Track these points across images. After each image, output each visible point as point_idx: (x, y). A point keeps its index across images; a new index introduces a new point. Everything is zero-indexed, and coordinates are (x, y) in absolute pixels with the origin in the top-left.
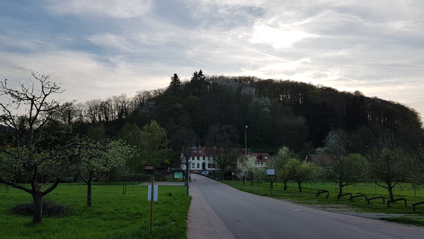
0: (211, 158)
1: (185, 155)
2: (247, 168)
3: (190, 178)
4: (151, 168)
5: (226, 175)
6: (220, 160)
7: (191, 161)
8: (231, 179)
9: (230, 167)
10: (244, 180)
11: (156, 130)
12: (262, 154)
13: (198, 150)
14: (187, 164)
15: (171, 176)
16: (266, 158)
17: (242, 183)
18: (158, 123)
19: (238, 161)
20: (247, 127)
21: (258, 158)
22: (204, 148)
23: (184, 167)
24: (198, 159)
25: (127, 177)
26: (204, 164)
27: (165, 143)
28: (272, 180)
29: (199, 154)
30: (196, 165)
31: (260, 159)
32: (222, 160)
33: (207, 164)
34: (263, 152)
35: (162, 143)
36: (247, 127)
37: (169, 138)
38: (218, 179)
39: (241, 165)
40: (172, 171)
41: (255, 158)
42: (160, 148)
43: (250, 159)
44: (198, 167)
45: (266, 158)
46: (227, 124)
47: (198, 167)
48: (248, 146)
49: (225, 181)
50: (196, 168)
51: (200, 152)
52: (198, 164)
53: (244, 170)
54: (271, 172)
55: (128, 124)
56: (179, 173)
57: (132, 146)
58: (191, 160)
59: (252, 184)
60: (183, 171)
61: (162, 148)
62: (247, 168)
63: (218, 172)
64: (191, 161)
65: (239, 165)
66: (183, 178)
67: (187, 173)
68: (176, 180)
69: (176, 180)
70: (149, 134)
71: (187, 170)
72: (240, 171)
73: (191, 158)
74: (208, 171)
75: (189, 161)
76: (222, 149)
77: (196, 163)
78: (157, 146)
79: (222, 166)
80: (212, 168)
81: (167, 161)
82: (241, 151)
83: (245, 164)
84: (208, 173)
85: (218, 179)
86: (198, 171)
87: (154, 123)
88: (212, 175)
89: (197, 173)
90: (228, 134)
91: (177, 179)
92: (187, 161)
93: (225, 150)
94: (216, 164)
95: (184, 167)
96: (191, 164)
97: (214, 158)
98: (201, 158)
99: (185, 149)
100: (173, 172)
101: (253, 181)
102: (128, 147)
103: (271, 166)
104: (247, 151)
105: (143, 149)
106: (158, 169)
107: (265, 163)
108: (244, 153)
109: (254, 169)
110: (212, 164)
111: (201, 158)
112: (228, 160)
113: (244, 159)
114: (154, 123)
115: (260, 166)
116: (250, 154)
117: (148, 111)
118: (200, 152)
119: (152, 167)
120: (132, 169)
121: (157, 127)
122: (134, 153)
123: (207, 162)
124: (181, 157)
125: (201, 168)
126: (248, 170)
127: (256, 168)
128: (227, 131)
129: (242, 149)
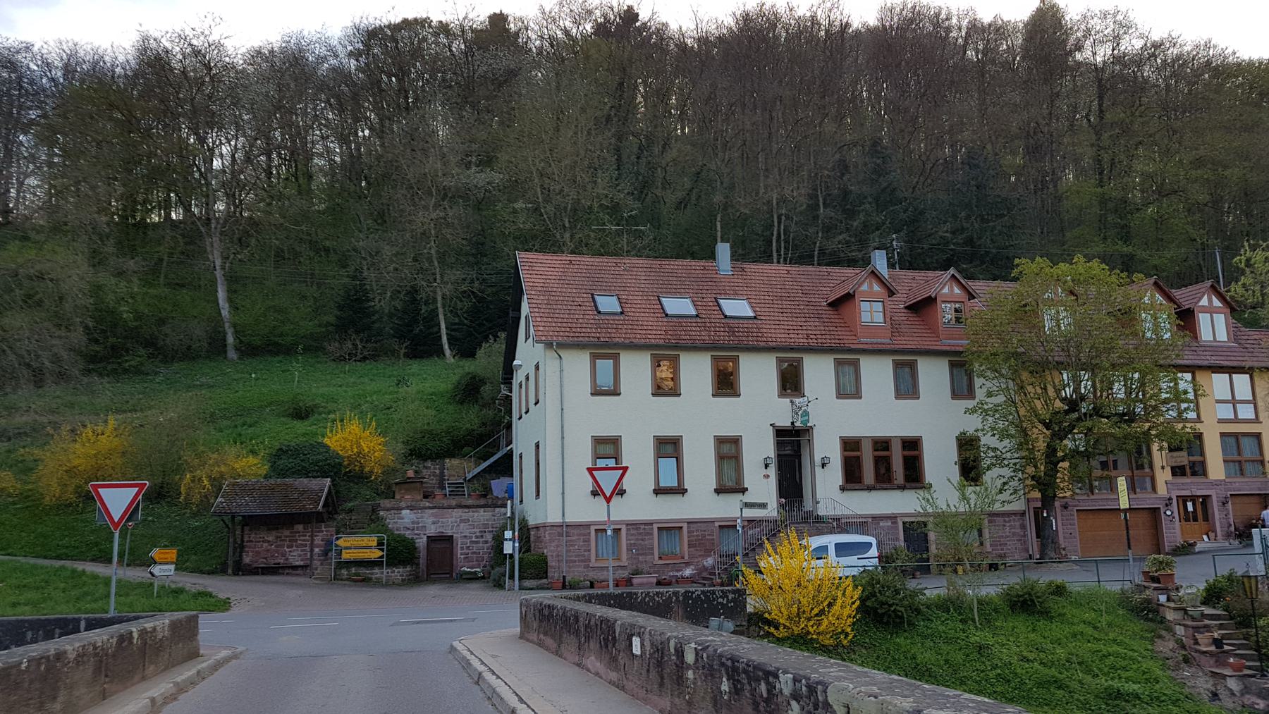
24: (726, 383)
30: (700, 467)
33: (825, 447)
44: (730, 485)
47: (730, 485)
51: (737, 307)
52: (729, 451)
98: (759, 373)
111: (759, 373)
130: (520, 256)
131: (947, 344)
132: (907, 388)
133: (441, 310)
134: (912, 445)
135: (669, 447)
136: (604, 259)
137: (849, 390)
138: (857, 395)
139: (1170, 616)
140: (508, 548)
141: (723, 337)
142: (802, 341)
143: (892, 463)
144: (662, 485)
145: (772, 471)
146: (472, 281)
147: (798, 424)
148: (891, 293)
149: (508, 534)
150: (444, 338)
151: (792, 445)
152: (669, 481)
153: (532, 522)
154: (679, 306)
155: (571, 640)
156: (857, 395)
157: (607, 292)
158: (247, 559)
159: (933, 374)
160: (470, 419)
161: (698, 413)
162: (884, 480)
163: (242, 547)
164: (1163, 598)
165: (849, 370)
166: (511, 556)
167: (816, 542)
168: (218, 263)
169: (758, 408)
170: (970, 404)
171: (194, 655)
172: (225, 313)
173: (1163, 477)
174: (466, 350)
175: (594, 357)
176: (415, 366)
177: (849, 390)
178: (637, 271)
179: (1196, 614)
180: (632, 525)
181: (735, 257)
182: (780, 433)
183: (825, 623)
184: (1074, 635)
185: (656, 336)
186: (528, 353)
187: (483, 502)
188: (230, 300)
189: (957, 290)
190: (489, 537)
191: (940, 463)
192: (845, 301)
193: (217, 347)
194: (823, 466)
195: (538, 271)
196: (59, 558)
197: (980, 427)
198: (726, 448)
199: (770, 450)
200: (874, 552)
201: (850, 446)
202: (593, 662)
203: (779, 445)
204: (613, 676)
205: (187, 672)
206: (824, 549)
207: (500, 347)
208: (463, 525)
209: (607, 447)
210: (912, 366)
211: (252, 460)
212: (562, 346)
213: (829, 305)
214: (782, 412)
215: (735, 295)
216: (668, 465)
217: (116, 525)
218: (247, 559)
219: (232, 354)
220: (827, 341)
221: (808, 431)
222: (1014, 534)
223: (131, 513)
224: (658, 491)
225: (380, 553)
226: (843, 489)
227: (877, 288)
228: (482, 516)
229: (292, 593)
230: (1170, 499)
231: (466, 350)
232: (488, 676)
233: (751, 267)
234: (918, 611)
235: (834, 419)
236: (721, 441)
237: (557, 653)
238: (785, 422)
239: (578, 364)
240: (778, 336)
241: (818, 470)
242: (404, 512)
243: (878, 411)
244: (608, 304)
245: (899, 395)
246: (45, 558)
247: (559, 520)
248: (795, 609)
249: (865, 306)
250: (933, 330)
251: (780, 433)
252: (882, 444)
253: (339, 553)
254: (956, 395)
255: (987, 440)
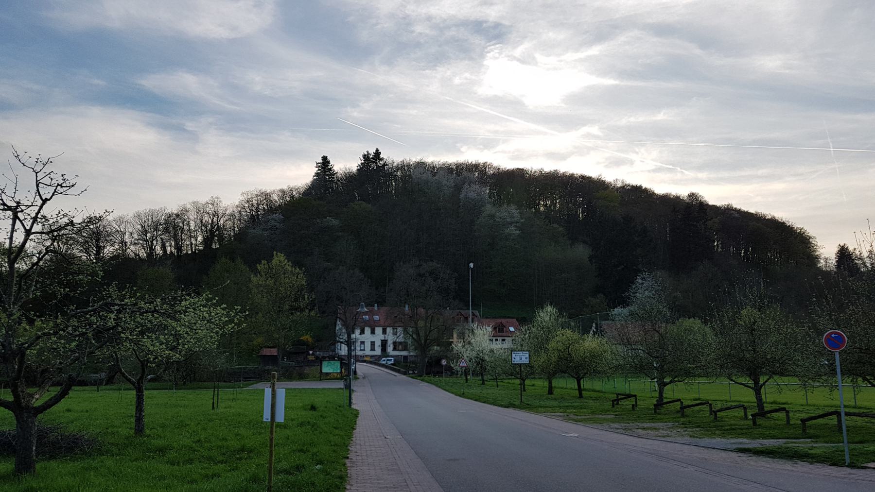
0: (400, 330)
1: (345, 324)
2: (472, 350)
3: (355, 373)
4: (274, 352)
5: (430, 364)
6: (418, 335)
7: (358, 336)
8: (439, 373)
9: (438, 348)
10: (466, 373)
11: (284, 274)
12: (504, 321)
13: (371, 313)
14: (350, 343)
15: (314, 370)
16: (512, 329)
17: (462, 380)
18: (288, 257)
19: (455, 336)
20: (472, 265)
21: (495, 328)
22: (384, 309)
23: (343, 350)
24: (373, 332)
25: (221, 371)
26: (384, 344)
27: (304, 298)
28: (524, 375)
29: (375, 321)
30: (368, 346)
31: (500, 331)
32: (422, 334)
34: (505, 317)
35: (296, 300)
36: (472, 265)
37: (311, 289)
38: (414, 373)
39: (460, 345)
40: (317, 358)
41: (490, 329)
42: (294, 309)
43: (479, 332)
44: (373, 349)
45: (512, 329)
46: (432, 261)
47: (373, 349)
48: (475, 306)
49: (427, 378)
50: (368, 352)
51: (377, 318)
52: (373, 344)
53: (467, 353)
54: (521, 358)
55: (223, 260)
56: (332, 362)
57: (230, 307)
58: (356, 334)
59: (483, 384)
60: (341, 359)
61: (296, 309)
62: (472, 350)
63: (413, 359)
64: (358, 336)
65: (457, 345)
66: (341, 372)
67: (349, 361)
68: (327, 377)
69: (327, 377)
70: (270, 282)
71: (349, 355)
72: (458, 357)
73: (358, 332)
74: (392, 356)
75: (353, 336)
76: (421, 310)
77: (368, 340)
78: (287, 307)
79: (422, 346)
80: (402, 350)
81: (307, 338)
82: (461, 315)
83: (469, 343)
84: (392, 362)
85: (414, 373)
86: (372, 356)
87: (279, 258)
88: (402, 366)
89: (371, 362)
90: (434, 281)
91: (327, 374)
92: (349, 336)
93: (427, 313)
94: (409, 342)
95: (343, 350)
96: (358, 344)
97: (405, 331)
98: (379, 330)
99: (345, 312)
100: (320, 361)
101: (485, 378)
102: (223, 309)
103: (522, 345)
104: (473, 314)
105: (257, 313)
106: (289, 355)
107: (510, 339)
108: (466, 318)
109: (487, 351)
110: (400, 343)
111: (379, 330)
112: (434, 334)
113: (467, 331)
114: (279, 258)
115: (500, 346)
116: (479, 322)
117: (266, 234)
118: (377, 318)
119: (276, 350)
120: (232, 354)
121: (287, 267)
122: (236, 321)
123: (391, 338)
124: (337, 328)
125: (378, 351)
126: (474, 354)
127: (492, 351)
128: (431, 273)
129: (463, 312)
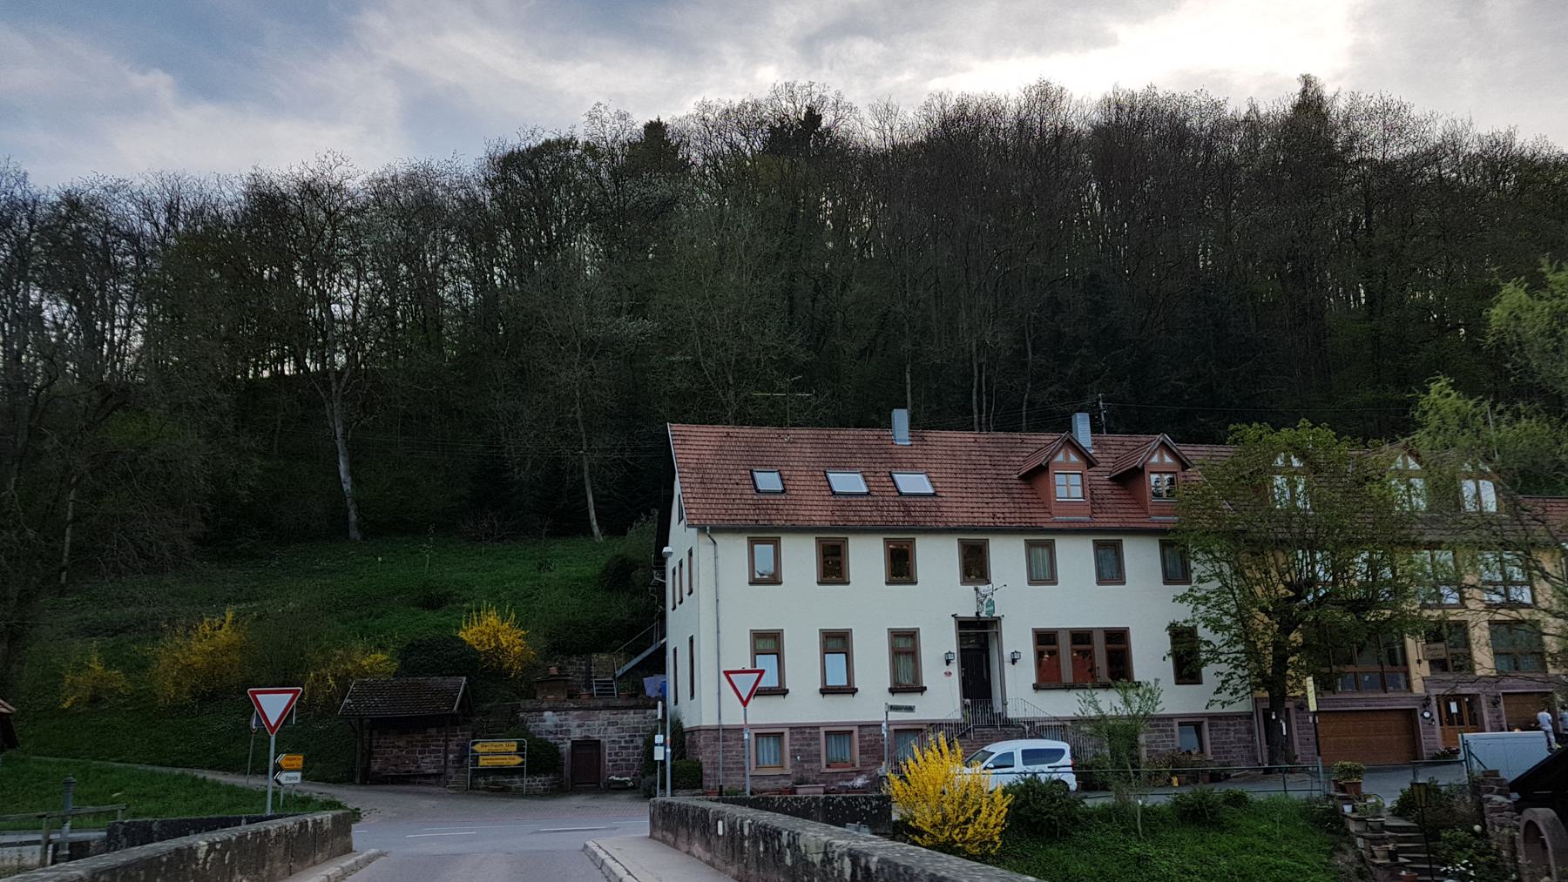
24: (901, 568)
26: (977, 638)
30: (872, 664)
33: (1016, 640)
44: (907, 683)
47: (907, 683)
51: (913, 483)
52: (905, 645)
98: (937, 558)
111: (937, 558)
125: (942, 697)
130: (672, 428)
131: (1157, 520)
132: (1110, 571)
133: (587, 481)
134: (1118, 639)
135: (837, 641)
136: (765, 430)
137: (1043, 574)
138: (1052, 580)
139: (1353, 827)
140: (659, 754)
141: (898, 516)
142: (987, 520)
143: (1094, 657)
144: (829, 683)
145: (955, 668)
146: (622, 450)
147: (983, 615)
148: (1090, 463)
149: (659, 739)
150: (592, 513)
151: (977, 638)
152: (837, 678)
153: (686, 725)
154: (848, 482)
155: (683, 831)
156: (1052, 580)
157: (768, 467)
158: (375, 767)
159: (1141, 557)
160: (621, 608)
161: (868, 601)
162: (1085, 679)
163: (370, 753)
164: (1348, 809)
165: (1042, 553)
166: (663, 763)
167: (998, 748)
168: (339, 431)
169: (938, 596)
170: (1182, 589)
171: (348, 850)
172: (347, 487)
173: (1420, 671)
174: (615, 526)
175: (752, 542)
176: (558, 547)
177: (1043, 574)
178: (801, 442)
179: (1376, 826)
180: (796, 729)
181: (914, 424)
182: (963, 624)
183: (970, 832)
184: (1245, 848)
185: (820, 517)
186: (681, 539)
187: (633, 702)
188: (351, 472)
189: (1168, 459)
190: (639, 741)
191: (1150, 658)
192: (1036, 476)
193: (337, 529)
194: (1014, 661)
195: (693, 445)
196: (175, 765)
197: (1190, 617)
198: (902, 643)
199: (952, 644)
200: (1067, 759)
201: (1045, 639)
202: (697, 848)
203: (962, 638)
204: (708, 856)
205: (348, 861)
206: (1010, 755)
207: (652, 526)
208: (606, 727)
209: (768, 642)
210: (1117, 548)
211: (380, 656)
212: (717, 530)
213: (1021, 478)
214: (965, 602)
215: (913, 468)
216: (836, 662)
217: (272, 730)
218: (375, 767)
219: (354, 533)
220: (1016, 520)
221: (994, 622)
222: (1240, 740)
223: (286, 716)
224: (826, 691)
225: (519, 760)
226: (1036, 687)
227: (1073, 458)
228: (631, 718)
229: (426, 804)
230: (1428, 699)
231: (615, 526)
232: (610, 862)
233: (933, 435)
234: (1075, 821)
235: (1024, 607)
236: (895, 634)
237: (675, 846)
238: (969, 612)
239: (734, 549)
240: (960, 516)
241: (1008, 666)
242: (547, 714)
243: (1077, 598)
244: (768, 481)
245: (1102, 580)
246: (161, 765)
247: (713, 722)
248: (939, 816)
249: (1060, 479)
250: (1141, 505)
251: (963, 624)
252: (1081, 637)
253: (476, 760)
254: (1168, 580)
255: (1204, 633)
